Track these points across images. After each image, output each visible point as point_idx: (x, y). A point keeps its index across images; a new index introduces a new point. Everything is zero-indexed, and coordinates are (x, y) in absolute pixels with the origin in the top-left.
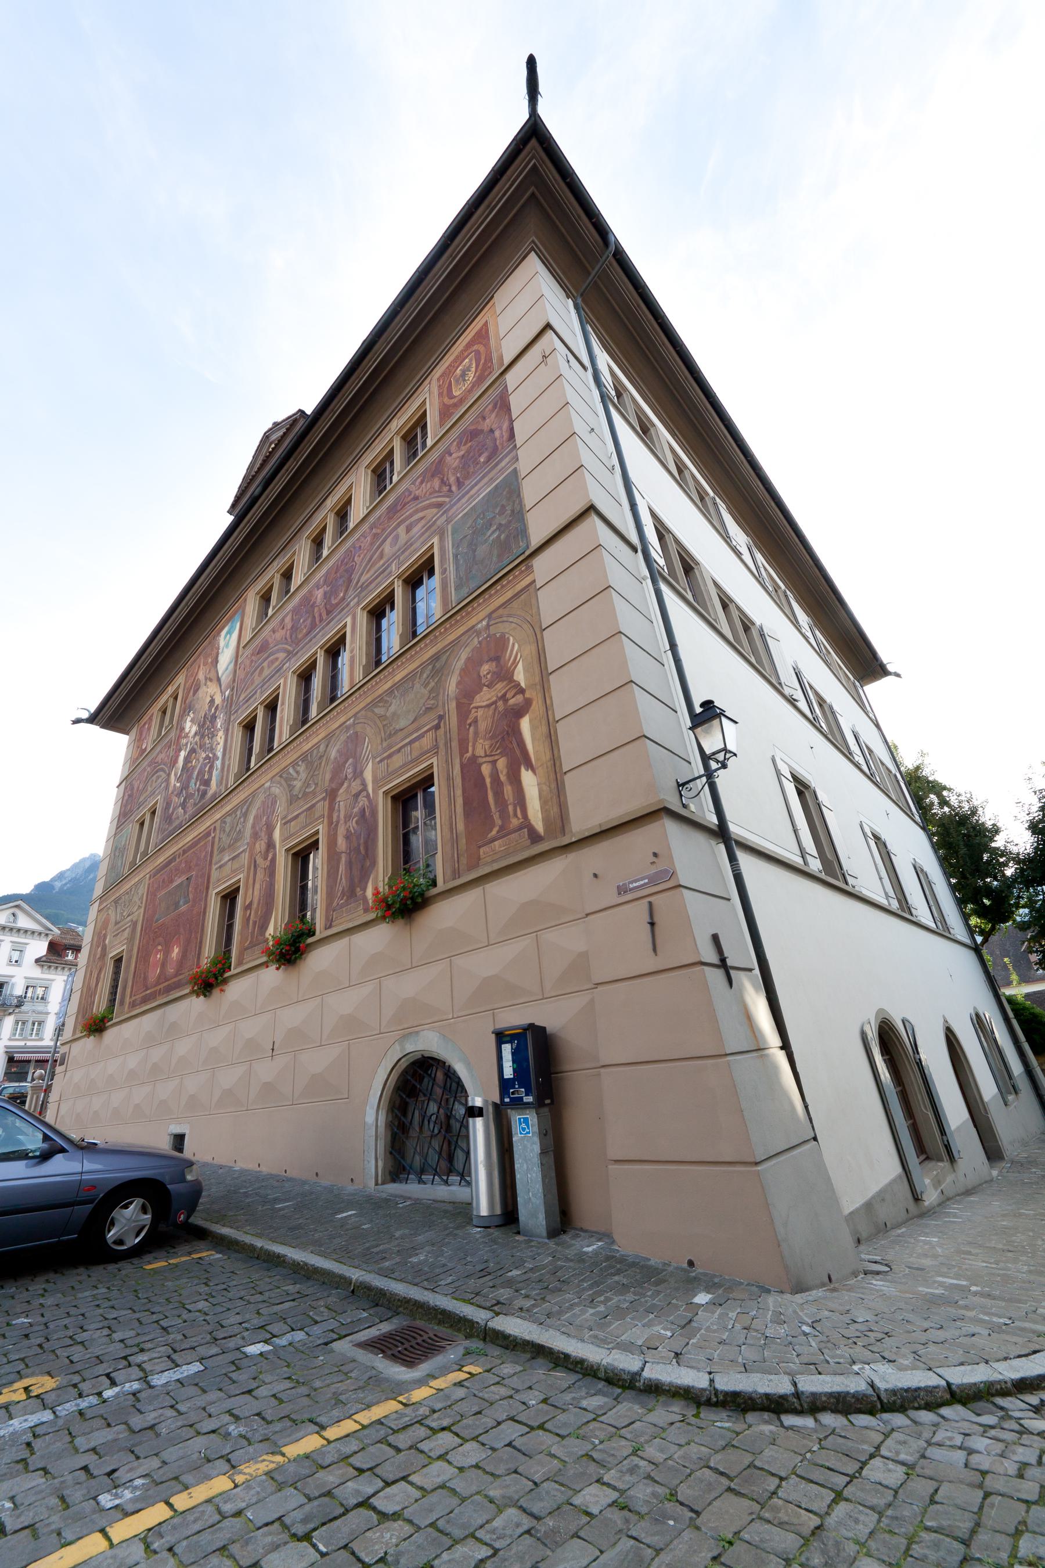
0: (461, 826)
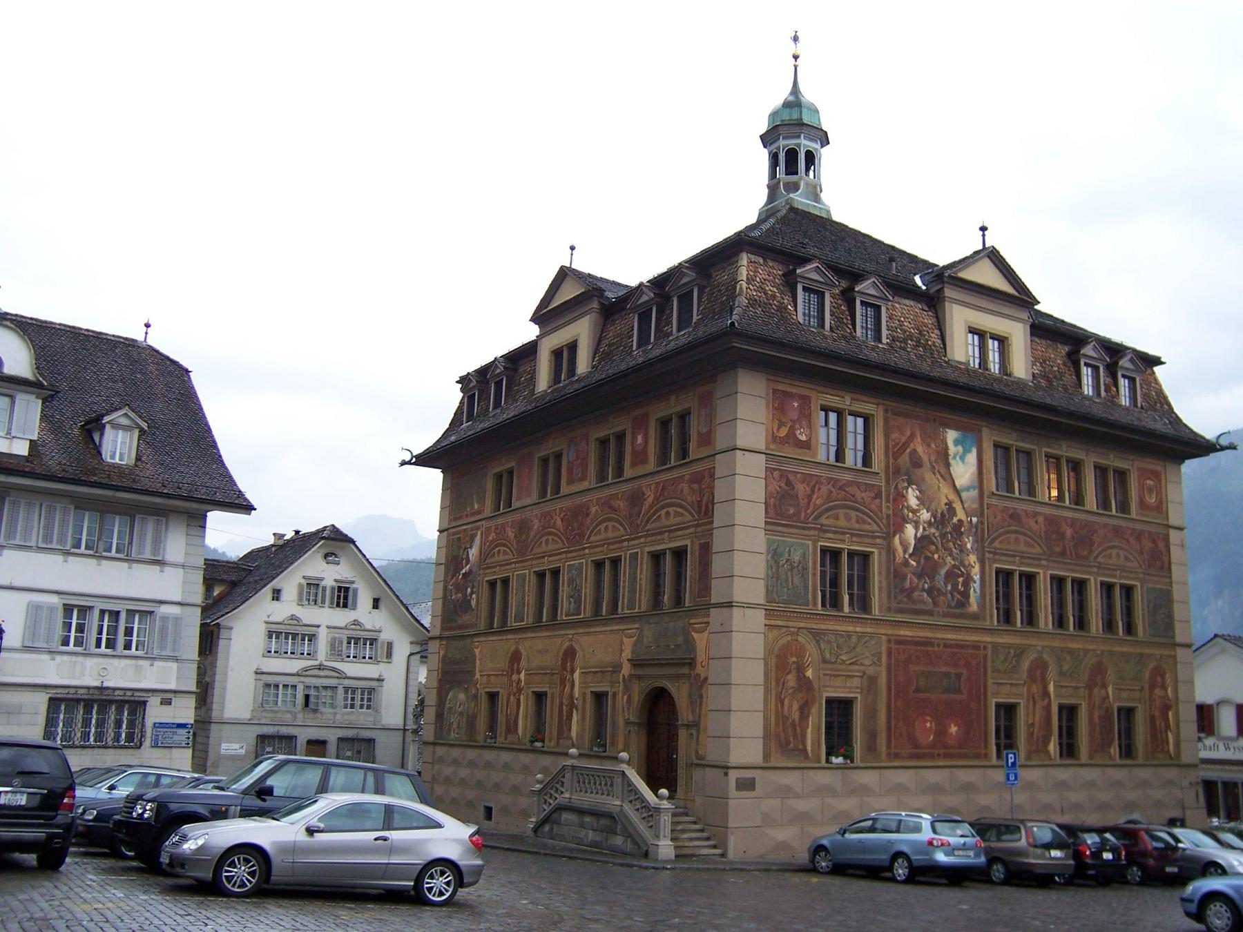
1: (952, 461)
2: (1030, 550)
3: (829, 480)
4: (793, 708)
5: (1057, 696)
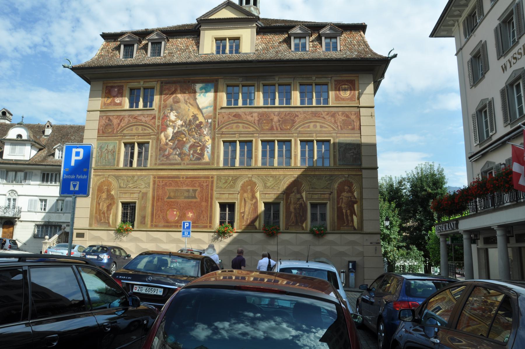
0: (336, 220)
2: (247, 130)
3: (129, 116)
4: (104, 207)
5: (261, 199)
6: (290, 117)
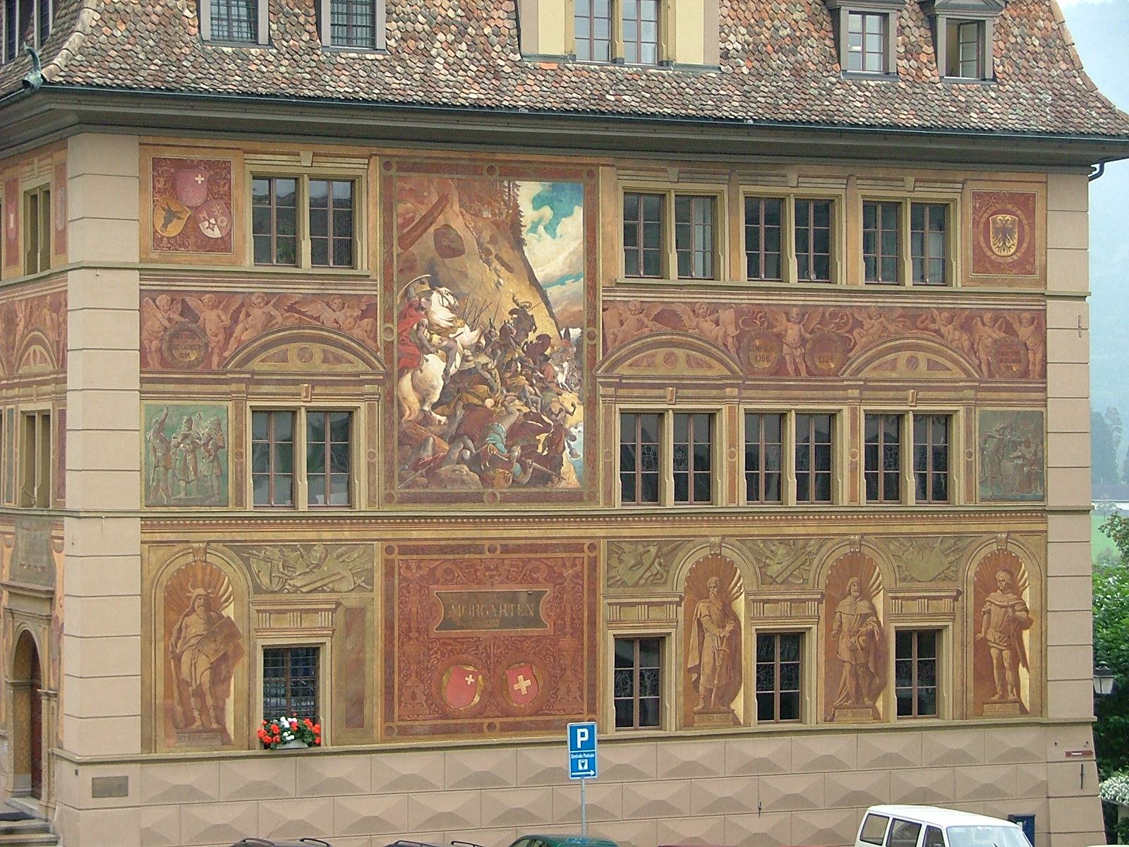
0: (971, 684)
1: (526, 235)
2: (700, 372)
4: (198, 668)
5: (751, 618)
6: (838, 326)
